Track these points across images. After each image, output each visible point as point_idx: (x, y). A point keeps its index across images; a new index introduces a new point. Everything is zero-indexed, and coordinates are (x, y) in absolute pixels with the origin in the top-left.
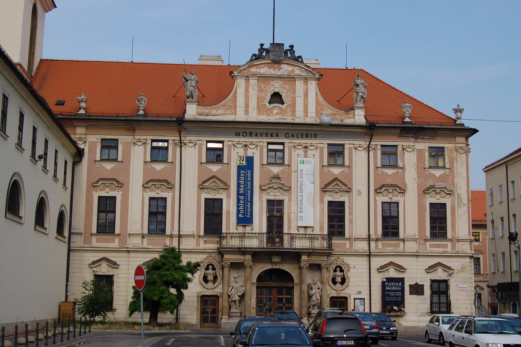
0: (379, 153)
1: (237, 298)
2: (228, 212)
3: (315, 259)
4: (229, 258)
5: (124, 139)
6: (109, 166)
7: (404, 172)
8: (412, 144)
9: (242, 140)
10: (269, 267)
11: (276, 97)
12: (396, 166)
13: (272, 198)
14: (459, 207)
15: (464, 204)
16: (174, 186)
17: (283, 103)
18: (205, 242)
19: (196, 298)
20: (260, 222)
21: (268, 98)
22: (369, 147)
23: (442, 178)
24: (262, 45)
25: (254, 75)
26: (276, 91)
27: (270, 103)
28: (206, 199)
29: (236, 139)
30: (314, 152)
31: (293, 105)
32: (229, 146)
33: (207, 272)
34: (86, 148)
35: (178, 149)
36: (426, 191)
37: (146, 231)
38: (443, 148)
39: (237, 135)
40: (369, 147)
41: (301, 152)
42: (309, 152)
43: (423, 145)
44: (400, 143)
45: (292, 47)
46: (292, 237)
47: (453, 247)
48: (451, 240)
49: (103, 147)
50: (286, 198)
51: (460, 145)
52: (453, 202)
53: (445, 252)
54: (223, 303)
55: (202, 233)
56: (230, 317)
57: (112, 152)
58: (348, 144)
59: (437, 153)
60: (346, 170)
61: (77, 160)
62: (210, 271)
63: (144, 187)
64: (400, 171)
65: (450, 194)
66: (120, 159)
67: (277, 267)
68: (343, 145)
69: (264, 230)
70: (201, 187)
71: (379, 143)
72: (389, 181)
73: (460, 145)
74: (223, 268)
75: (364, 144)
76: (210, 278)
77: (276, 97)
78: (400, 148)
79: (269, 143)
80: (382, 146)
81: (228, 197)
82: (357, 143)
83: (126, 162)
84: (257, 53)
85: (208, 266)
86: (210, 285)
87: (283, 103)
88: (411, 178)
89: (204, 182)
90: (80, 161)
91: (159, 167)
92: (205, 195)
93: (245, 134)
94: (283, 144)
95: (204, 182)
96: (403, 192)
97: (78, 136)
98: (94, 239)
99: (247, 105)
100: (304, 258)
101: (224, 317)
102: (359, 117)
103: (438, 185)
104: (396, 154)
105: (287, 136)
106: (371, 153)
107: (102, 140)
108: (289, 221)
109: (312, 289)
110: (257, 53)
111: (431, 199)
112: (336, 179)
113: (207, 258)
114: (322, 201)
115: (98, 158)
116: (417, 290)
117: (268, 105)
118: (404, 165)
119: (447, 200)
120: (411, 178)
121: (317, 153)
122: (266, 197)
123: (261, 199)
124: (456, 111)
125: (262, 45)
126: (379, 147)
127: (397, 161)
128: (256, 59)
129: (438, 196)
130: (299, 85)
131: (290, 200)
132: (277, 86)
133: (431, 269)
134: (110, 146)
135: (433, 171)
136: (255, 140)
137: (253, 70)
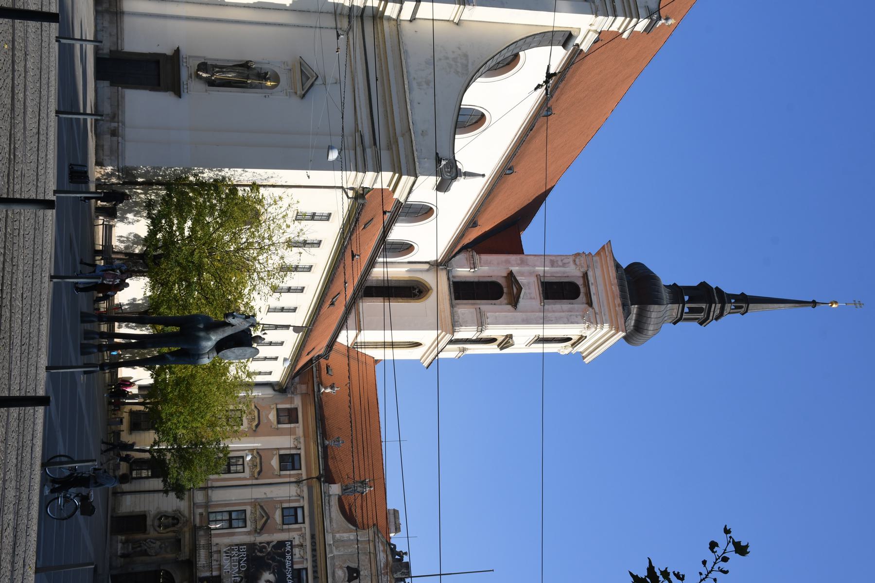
2: (233, 534)
4: (187, 538)
5: (299, 428)
6: (272, 416)
16: (257, 479)
18: (201, 514)
19: (142, 509)
26: (362, 573)
27: (348, 568)
29: (308, 536)
32: (300, 529)
35: (293, 480)
39: (313, 537)
49: (289, 410)
54: (139, 536)
55: (210, 510)
56: (123, 543)
57: (286, 419)
61: (276, 388)
62: (170, 520)
66: (280, 426)
70: (257, 504)
74: (174, 531)
81: (249, 533)
83: (278, 432)
84: (398, 549)
85: (177, 519)
89: (261, 507)
91: (275, 462)
92: (249, 509)
93: (313, 544)
95: (261, 507)
97: (298, 386)
101: (123, 538)
107: (296, 409)
110: (398, 549)
113: (184, 517)
115: (280, 406)
128: (391, 549)
134: (291, 416)
136: (309, 556)
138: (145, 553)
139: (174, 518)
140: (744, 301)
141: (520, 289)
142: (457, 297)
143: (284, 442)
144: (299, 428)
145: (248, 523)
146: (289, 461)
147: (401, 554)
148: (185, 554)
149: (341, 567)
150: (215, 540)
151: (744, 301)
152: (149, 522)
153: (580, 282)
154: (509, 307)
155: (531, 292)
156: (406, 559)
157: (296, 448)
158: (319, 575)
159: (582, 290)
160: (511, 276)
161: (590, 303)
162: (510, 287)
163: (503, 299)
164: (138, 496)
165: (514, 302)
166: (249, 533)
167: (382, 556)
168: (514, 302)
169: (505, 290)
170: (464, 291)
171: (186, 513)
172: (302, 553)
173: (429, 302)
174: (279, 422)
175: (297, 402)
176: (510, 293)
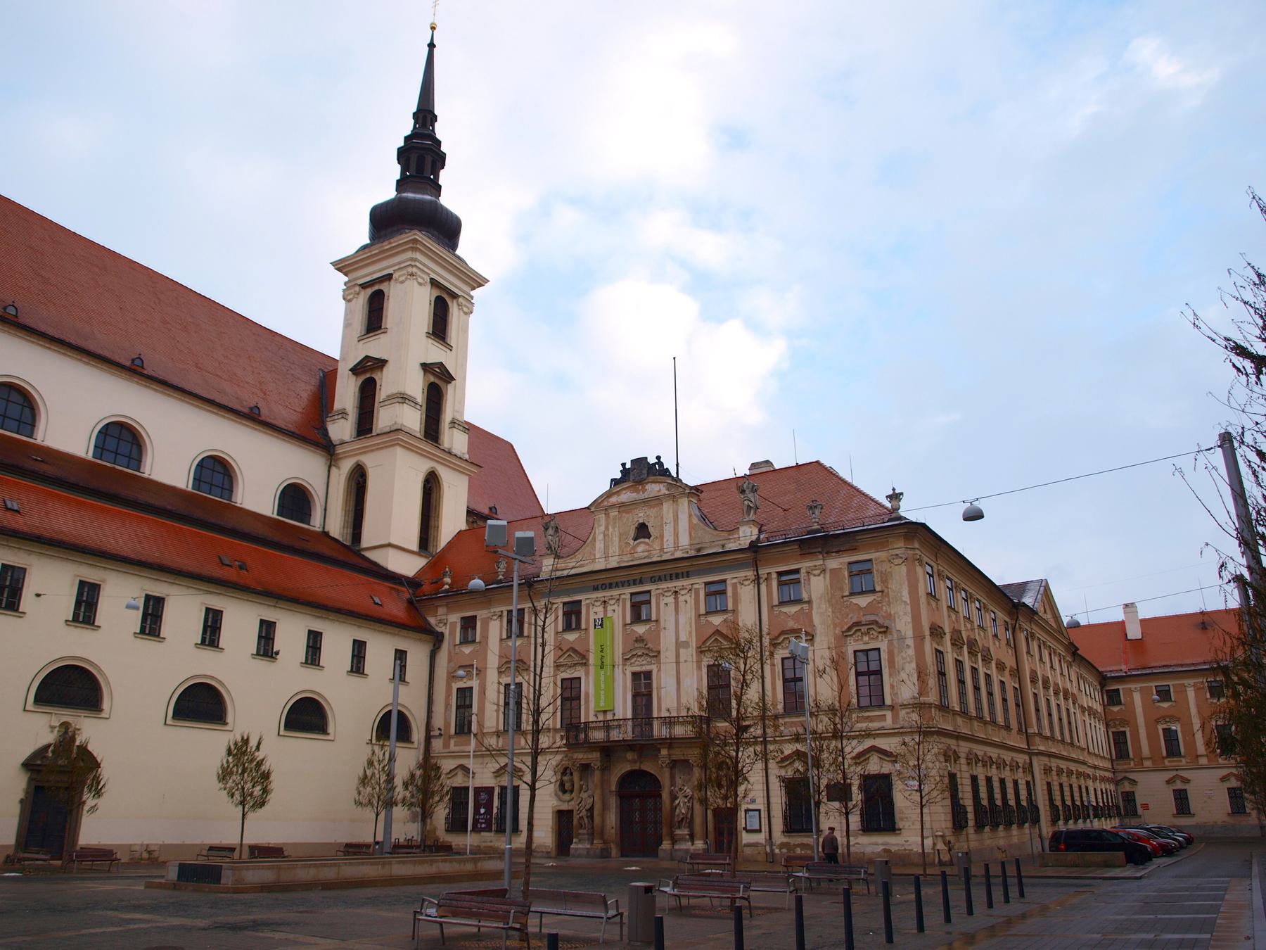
0: (775, 584)
1: (584, 813)
2: (587, 695)
3: (678, 754)
5: (481, 614)
6: (467, 650)
7: (811, 608)
8: (821, 562)
9: (600, 594)
10: (628, 767)
11: (642, 531)
12: (799, 601)
13: (638, 669)
14: (900, 651)
15: (908, 646)
17: (649, 536)
20: (623, 707)
21: (632, 533)
22: (758, 578)
23: (870, 608)
24: (623, 465)
25: (613, 506)
28: (563, 680)
30: (687, 597)
31: (662, 537)
33: (565, 778)
34: (446, 631)
36: (846, 634)
37: (501, 728)
38: (870, 560)
39: (596, 589)
40: (758, 578)
41: (671, 600)
42: (681, 599)
43: (835, 563)
44: (804, 565)
45: (658, 458)
46: (670, 722)
47: (895, 717)
48: (892, 708)
50: (654, 668)
51: (896, 552)
52: (890, 641)
53: (882, 728)
58: (731, 577)
59: (861, 572)
60: (729, 616)
63: (500, 673)
64: (806, 606)
65: (885, 631)
67: (636, 767)
68: (724, 581)
69: (629, 715)
71: (773, 570)
72: (791, 624)
73: (896, 552)
75: (750, 574)
76: (567, 786)
77: (642, 531)
78: (803, 571)
79: (632, 594)
80: (780, 574)
81: (587, 674)
82: (741, 574)
84: (619, 476)
85: (566, 769)
86: (567, 796)
87: (649, 536)
88: (822, 617)
90: (439, 647)
93: (604, 587)
94: (649, 592)
96: (811, 638)
98: (452, 742)
99: (606, 547)
100: (664, 752)
102: (747, 534)
103: (864, 619)
104: (798, 581)
105: (653, 580)
106: (763, 587)
108: (659, 699)
109: (676, 798)
110: (619, 476)
111: (852, 646)
112: (717, 632)
114: (699, 668)
115: (458, 642)
116: (840, 792)
117: (631, 542)
118: (810, 597)
119: (883, 645)
120: (822, 617)
121: (690, 598)
122: (629, 670)
123: (624, 674)
124: (890, 497)
125: (623, 465)
126: (774, 576)
127: (800, 593)
129: (866, 638)
130: (667, 507)
131: (659, 670)
132: (641, 515)
133: (861, 757)
135: (855, 600)
136: (615, 593)
137: (614, 500)
138: (591, 810)
139: (564, 773)
140: (425, 115)
141: (367, 358)
142: (370, 431)
143: (495, 630)
144: (481, 614)
145: (576, 675)
146: (516, 625)
147: (625, 472)
148: (594, 757)
149: (634, 548)
150: (592, 718)
151: (425, 115)
152: (565, 807)
153: (370, 291)
154: (385, 369)
155: (376, 347)
156: (628, 466)
157: (501, 616)
158: (638, 577)
159: (376, 288)
160: (356, 370)
161: (389, 277)
162: (365, 372)
163: (376, 376)
164: (536, 822)
165: (380, 364)
166: (587, 674)
167: (626, 496)
168: (380, 364)
169: (368, 375)
170: (365, 425)
171: (559, 757)
172: (612, 602)
173: (369, 461)
174: (474, 641)
175: (455, 618)
176: (372, 369)
